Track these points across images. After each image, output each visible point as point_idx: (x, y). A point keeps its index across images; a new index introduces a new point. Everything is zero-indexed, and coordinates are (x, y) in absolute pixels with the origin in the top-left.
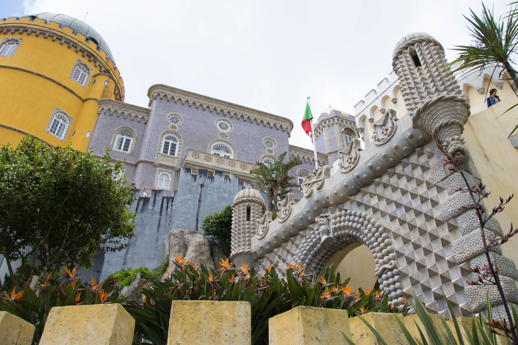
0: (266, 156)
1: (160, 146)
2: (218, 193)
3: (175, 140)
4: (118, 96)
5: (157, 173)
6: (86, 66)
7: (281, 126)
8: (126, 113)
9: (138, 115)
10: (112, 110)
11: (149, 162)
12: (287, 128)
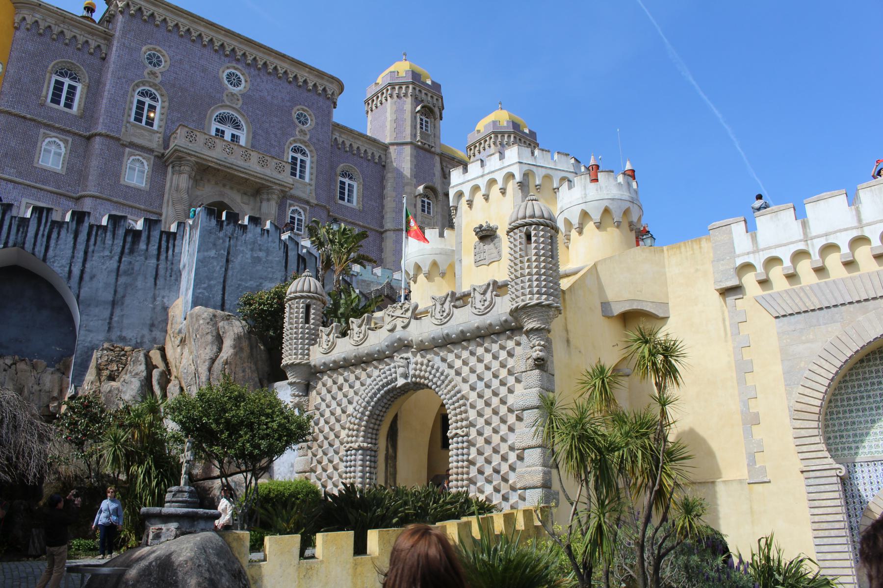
0: (295, 141)
1: (131, 109)
2: (252, 250)
3: (154, 98)
5: (126, 158)
7: (324, 90)
9: (90, 41)
12: (333, 94)
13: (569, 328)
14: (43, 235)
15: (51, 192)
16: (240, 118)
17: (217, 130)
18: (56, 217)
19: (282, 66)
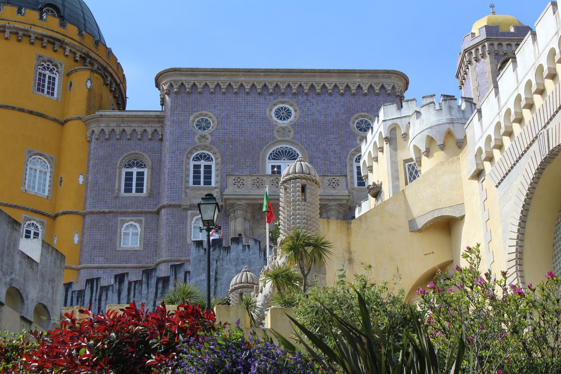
1: (188, 176)
2: (236, 265)
3: (208, 158)
4: (114, 85)
5: (189, 220)
6: (51, 62)
8: (129, 131)
9: (147, 129)
10: (107, 131)
11: (174, 206)
13: (352, 249)
14: (96, 300)
15: (134, 268)
16: (294, 148)
17: (273, 167)
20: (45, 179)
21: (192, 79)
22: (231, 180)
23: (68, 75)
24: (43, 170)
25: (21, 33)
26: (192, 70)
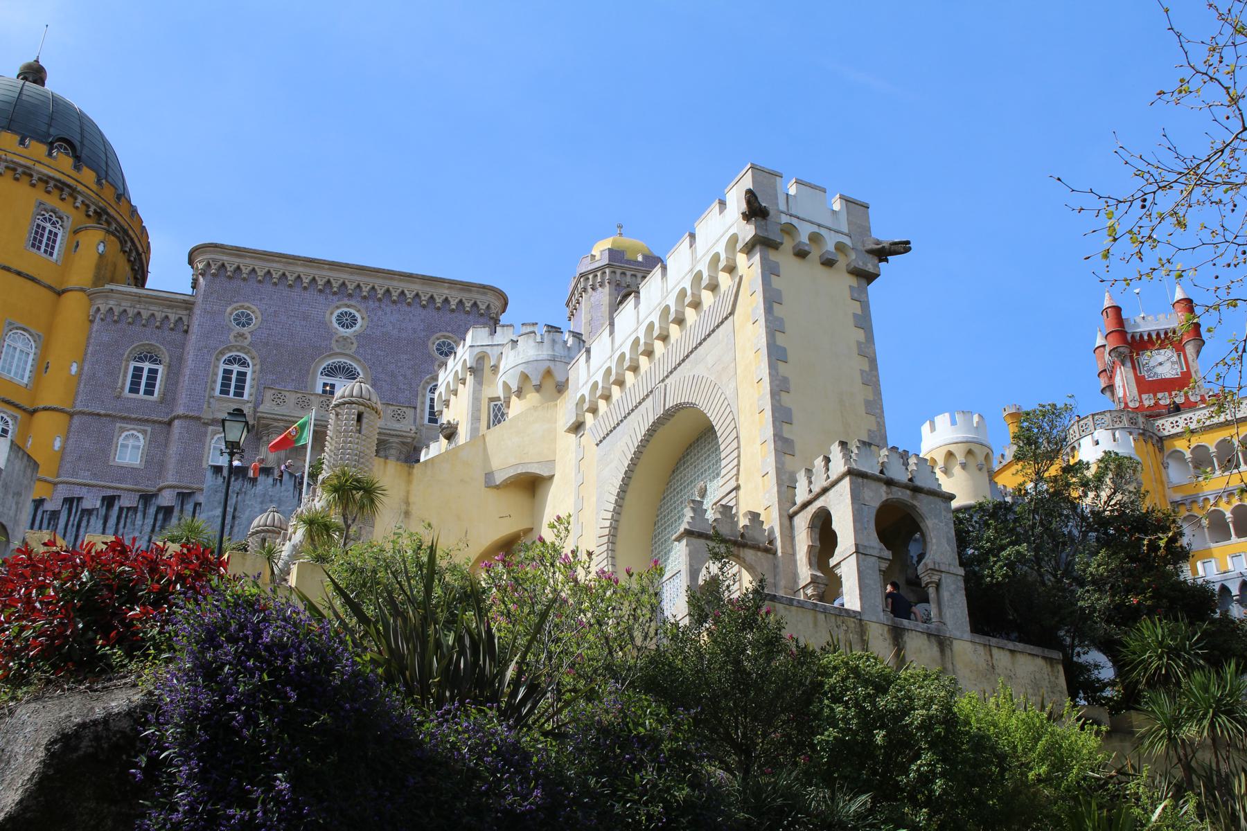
1: (215, 382)
2: (262, 503)
3: (243, 363)
4: (134, 254)
5: (209, 438)
8: (145, 314)
10: (117, 311)
11: (192, 418)
15: (129, 490)
17: (325, 385)
18: (86, 504)
19: (411, 289)
20: (26, 362)
21: (237, 261)
22: (269, 395)
23: (76, 232)
24: (26, 350)
25: (20, 170)
26: (238, 249)
